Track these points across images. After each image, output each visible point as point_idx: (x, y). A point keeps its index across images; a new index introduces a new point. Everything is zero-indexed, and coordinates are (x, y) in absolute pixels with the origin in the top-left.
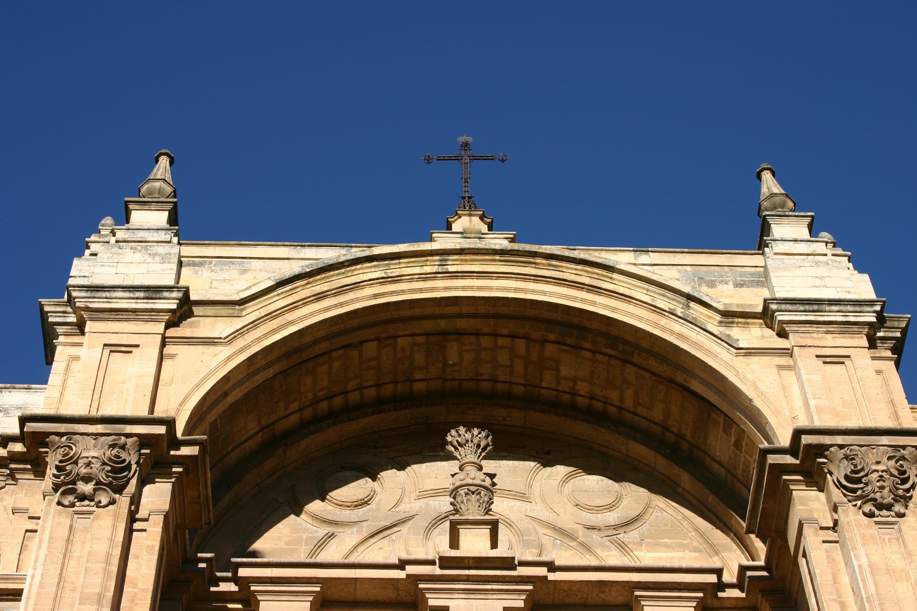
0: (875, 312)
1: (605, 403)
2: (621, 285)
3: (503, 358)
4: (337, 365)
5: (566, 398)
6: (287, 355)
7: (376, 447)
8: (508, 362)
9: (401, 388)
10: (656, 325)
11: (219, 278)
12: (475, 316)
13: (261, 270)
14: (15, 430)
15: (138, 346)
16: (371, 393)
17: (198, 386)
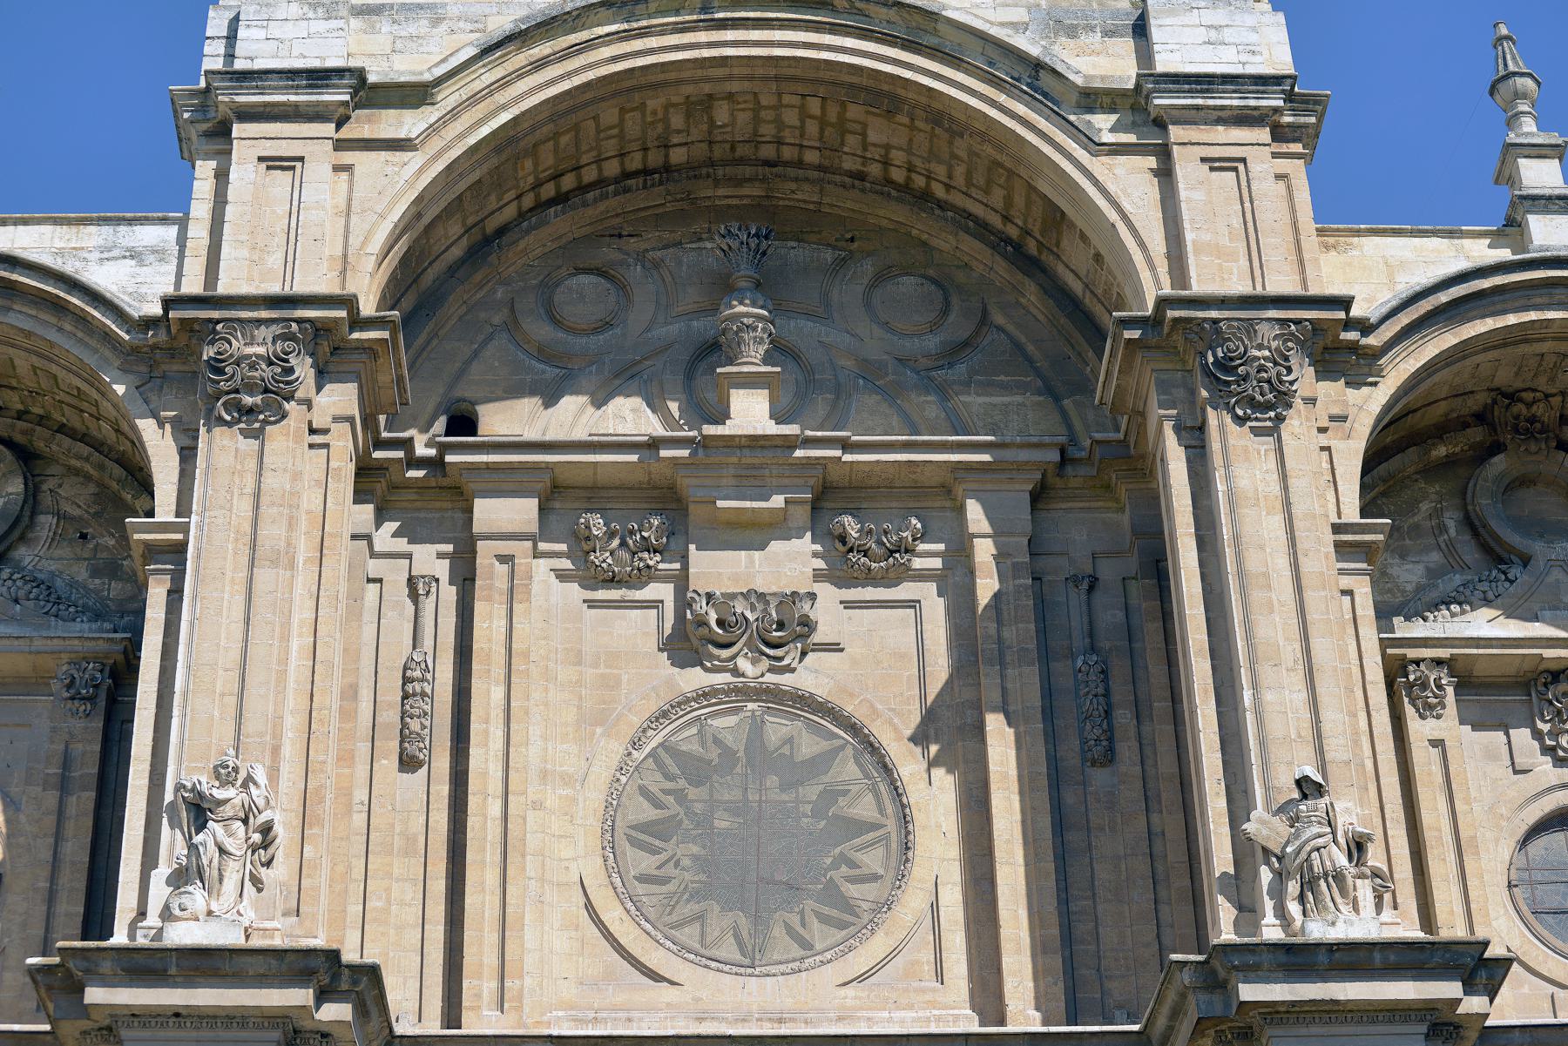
0: (1283, 92)
1: (928, 177)
2: (950, 39)
3: (791, 117)
4: (565, 140)
5: (875, 170)
6: (498, 150)
7: (620, 236)
8: (797, 123)
9: (655, 159)
10: (993, 103)
11: (403, 33)
12: (751, 78)
13: (459, 19)
14: (157, 310)
15: (301, 159)
16: (612, 169)
17: (382, 216)
